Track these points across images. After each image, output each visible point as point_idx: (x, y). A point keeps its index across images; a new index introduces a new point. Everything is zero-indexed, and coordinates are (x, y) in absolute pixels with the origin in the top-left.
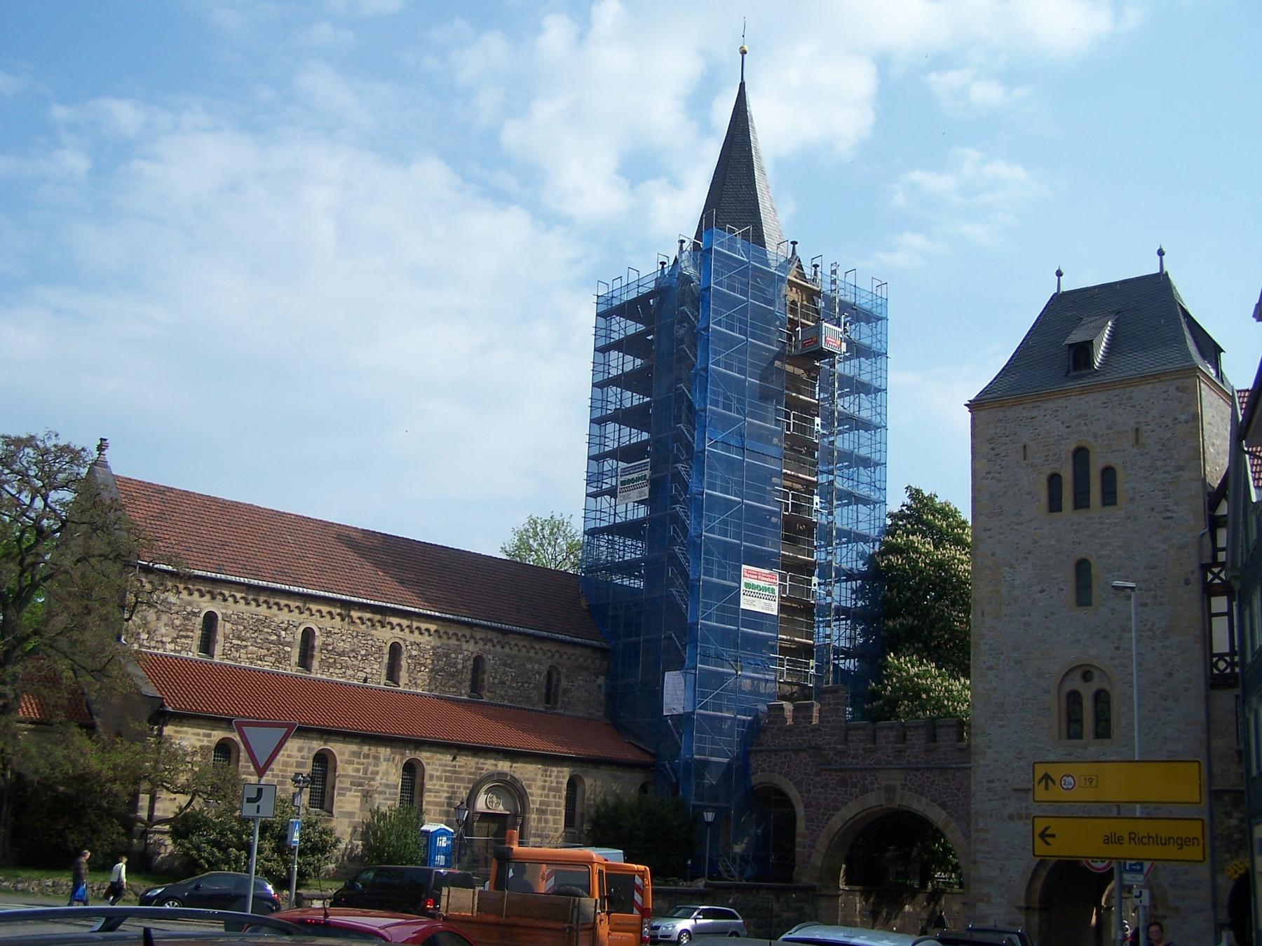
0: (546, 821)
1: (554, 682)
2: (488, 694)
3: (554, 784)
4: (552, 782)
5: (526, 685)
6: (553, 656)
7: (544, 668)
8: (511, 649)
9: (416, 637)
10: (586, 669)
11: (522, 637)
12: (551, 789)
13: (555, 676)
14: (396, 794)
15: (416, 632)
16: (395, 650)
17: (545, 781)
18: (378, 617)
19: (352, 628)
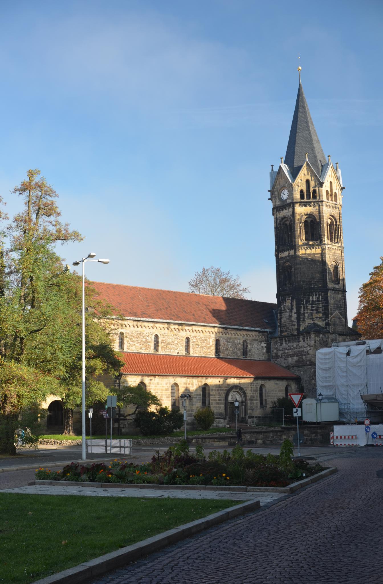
0: (253, 404)
1: (245, 347)
2: (222, 354)
3: (255, 389)
4: (254, 388)
5: (235, 349)
6: (244, 336)
7: (241, 342)
8: (229, 335)
9: (195, 334)
10: (257, 340)
11: (233, 330)
12: (254, 391)
13: (245, 344)
14: (200, 398)
15: (195, 332)
16: (188, 339)
17: (252, 388)
18: (180, 327)
19: (171, 333)
